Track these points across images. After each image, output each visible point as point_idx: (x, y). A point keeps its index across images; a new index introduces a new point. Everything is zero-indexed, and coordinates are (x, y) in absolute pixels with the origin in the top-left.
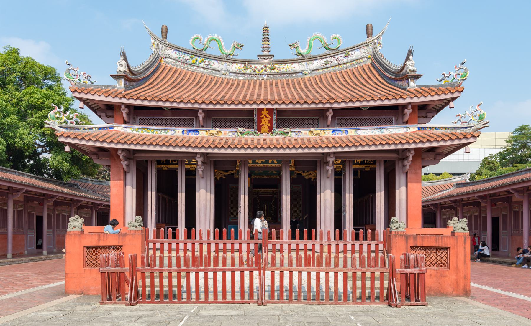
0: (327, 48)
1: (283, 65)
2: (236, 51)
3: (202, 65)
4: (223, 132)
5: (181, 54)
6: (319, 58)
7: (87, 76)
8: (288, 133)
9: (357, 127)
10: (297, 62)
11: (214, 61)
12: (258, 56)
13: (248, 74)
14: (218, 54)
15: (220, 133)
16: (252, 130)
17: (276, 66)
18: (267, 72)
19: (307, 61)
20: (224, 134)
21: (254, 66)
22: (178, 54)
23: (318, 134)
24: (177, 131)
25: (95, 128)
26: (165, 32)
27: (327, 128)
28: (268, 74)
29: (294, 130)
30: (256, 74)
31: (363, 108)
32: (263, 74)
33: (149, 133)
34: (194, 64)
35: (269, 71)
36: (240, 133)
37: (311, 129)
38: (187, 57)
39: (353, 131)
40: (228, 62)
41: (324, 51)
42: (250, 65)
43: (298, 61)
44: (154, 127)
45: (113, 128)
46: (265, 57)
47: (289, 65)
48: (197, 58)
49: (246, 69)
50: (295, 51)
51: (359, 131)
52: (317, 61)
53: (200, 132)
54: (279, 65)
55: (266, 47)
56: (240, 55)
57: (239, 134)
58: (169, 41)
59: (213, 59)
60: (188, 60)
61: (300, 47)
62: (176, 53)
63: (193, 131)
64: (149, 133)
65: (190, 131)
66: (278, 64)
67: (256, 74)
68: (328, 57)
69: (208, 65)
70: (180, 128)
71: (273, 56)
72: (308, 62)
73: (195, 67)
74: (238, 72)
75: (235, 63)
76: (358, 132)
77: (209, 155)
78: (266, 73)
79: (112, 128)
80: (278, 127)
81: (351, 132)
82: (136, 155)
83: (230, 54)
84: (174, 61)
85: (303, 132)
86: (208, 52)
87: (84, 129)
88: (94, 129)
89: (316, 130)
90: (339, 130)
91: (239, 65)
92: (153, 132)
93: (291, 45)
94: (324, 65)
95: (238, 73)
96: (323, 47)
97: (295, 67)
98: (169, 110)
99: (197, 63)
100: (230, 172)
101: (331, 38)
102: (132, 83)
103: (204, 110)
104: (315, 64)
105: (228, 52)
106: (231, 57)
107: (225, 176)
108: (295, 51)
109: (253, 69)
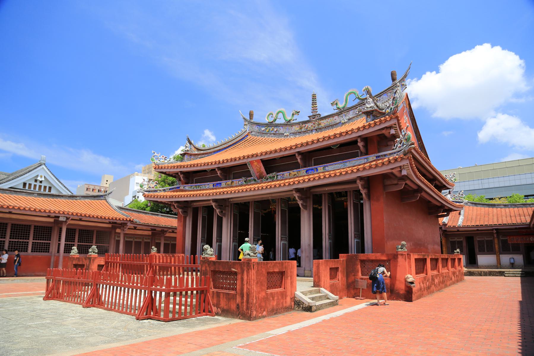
0: (358, 98)
1: (327, 119)
2: (295, 117)
3: (273, 132)
4: (235, 182)
5: (260, 127)
6: (353, 108)
7: (164, 157)
8: (275, 176)
9: (325, 165)
10: (337, 115)
11: (280, 128)
12: (309, 117)
13: (302, 132)
14: (282, 121)
15: (233, 183)
16: (252, 178)
17: (322, 121)
18: (316, 127)
19: (344, 113)
20: (236, 183)
21: (307, 125)
22: (259, 128)
23: (296, 174)
24: (210, 185)
25: (167, 189)
26: (251, 115)
27: (302, 169)
28: (316, 129)
29: (278, 174)
30: (308, 131)
31: (333, 146)
32: (313, 130)
33: (197, 188)
34: (268, 133)
35: (316, 127)
36: (245, 181)
37: (289, 171)
38: (263, 129)
39: (322, 168)
40: (289, 126)
41: (357, 101)
42: (304, 125)
43: (338, 114)
44: (199, 184)
45: (179, 188)
46: (313, 117)
47: (331, 118)
48: (270, 127)
49: (301, 129)
50: (335, 107)
51: (327, 167)
52: (353, 111)
53: (222, 184)
54: (324, 120)
55: (314, 109)
56: (299, 119)
57: (244, 183)
58: (252, 121)
59: (279, 126)
60: (264, 130)
61: (339, 103)
62: (258, 128)
63: (219, 184)
64: (197, 188)
65: (217, 184)
66: (323, 120)
67: (308, 131)
68: (361, 106)
69: (276, 131)
70: (211, 183)
71: (319, 114)
72: (345, 113)
73: (268, 134)
74: (296, 132)
75: (293, 125)
76: (327, 168)
77: (229, 200)
78: (315, 128)
79: (179, 187)
80: (268, 174)
81: (321, 169)
82: (193, 204)
83: (290, 121)
84: (256, 133)
85: (285, 174)
86: (278, 122)
87: (160, 191)
88: (166, 190)
89: (293, 172)
90: (311, 169)
91: (296, 126)
92: (199, 187)
93: (332, 103)
94: (357, 113)
95: (296, 133)
96: (357, 99)
97: (335, 119)
98: (210, 171)
99: (270, 131)
100: (267, 210)
101: (363, 91)
102: (192, 157)
103: (219, 168)
104: (351, 114)
105: (289, 118)
106: (292, 122)
107: (264, 214)
108: (335, 107)
109: (306, 127)
